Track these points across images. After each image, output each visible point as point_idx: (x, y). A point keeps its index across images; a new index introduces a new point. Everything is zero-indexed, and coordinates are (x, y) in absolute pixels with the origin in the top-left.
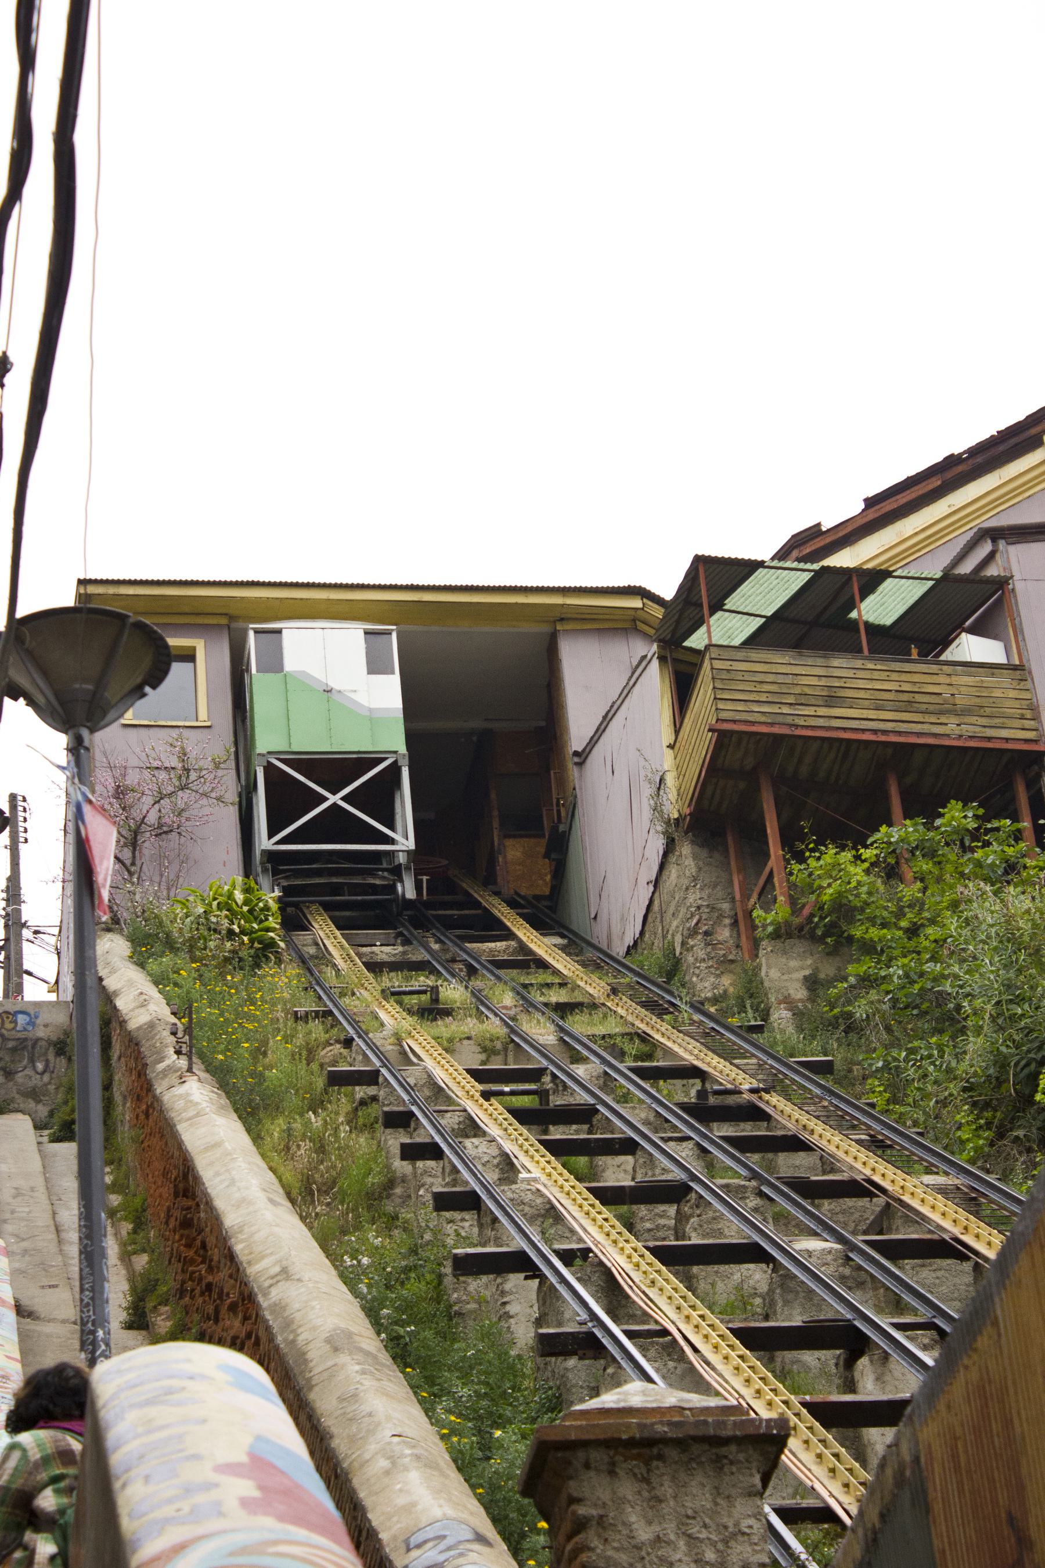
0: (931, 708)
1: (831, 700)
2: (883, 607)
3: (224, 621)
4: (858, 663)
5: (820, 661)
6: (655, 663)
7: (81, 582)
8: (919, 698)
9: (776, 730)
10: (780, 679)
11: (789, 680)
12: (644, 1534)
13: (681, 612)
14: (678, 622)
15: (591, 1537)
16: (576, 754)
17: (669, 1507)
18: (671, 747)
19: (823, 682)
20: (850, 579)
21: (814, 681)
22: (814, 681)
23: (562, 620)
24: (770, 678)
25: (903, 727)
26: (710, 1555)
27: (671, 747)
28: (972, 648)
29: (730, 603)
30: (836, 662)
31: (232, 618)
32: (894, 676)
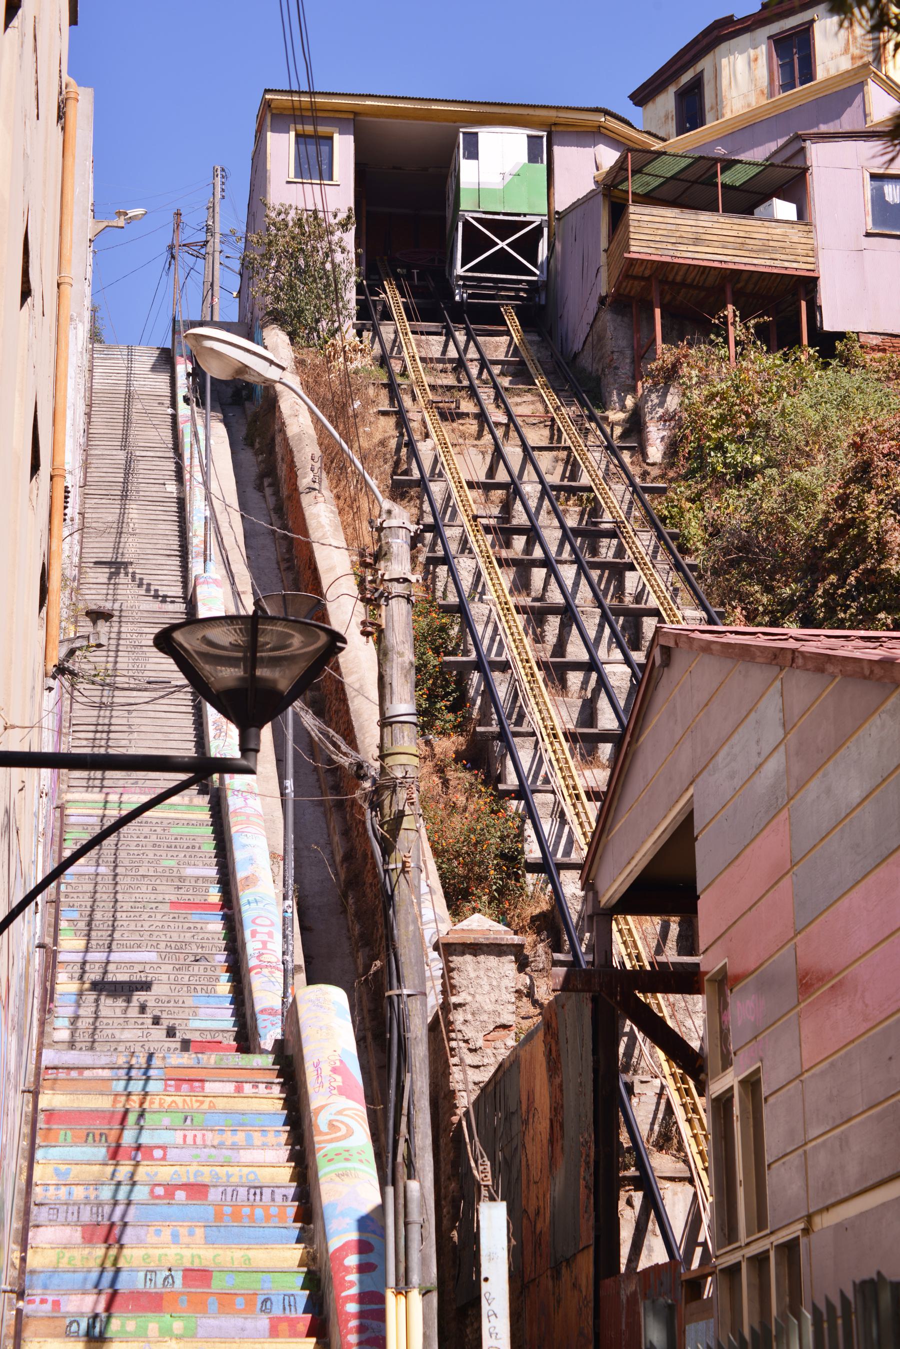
0: (755, 248)
1: (697, 241)
2: (736, 177)
3: (351, 116)
4: (715, 218)
5: (693, 216)
6: (600, 198)
7: (267, 91)
8: (748, 241)
9: (664, 259)
10: (669, 227)
11: (673, 227)
12: (473, 975)
13: (617, 172)
14: (615, 177)
15: (454, 974)
16: (557, 213)
17: (482, 965)
18: (605, 251)
19: (694, 229)
20: (716, 164)
21: (688, 229)
22: (688, 229)
23: (555, 124)
24: (663, 226)
25: (737, 259)
26: (495, 983)
27: (605, 251)
28: (784, 209)
29: (645, 170)
30: (702, 217)
31: (356, 114)
32: (735, 227)
